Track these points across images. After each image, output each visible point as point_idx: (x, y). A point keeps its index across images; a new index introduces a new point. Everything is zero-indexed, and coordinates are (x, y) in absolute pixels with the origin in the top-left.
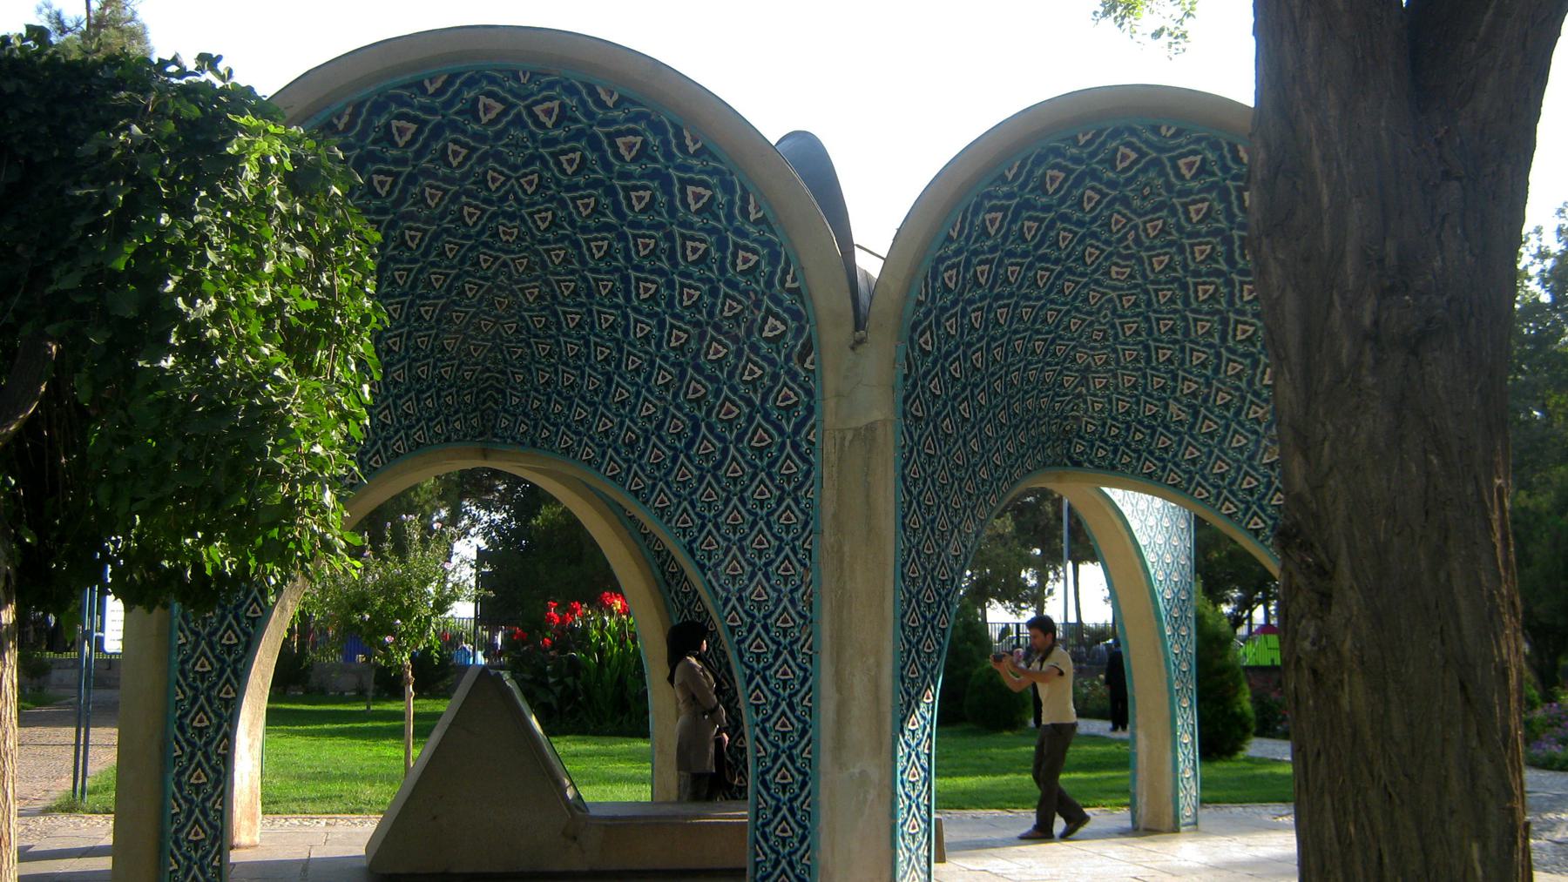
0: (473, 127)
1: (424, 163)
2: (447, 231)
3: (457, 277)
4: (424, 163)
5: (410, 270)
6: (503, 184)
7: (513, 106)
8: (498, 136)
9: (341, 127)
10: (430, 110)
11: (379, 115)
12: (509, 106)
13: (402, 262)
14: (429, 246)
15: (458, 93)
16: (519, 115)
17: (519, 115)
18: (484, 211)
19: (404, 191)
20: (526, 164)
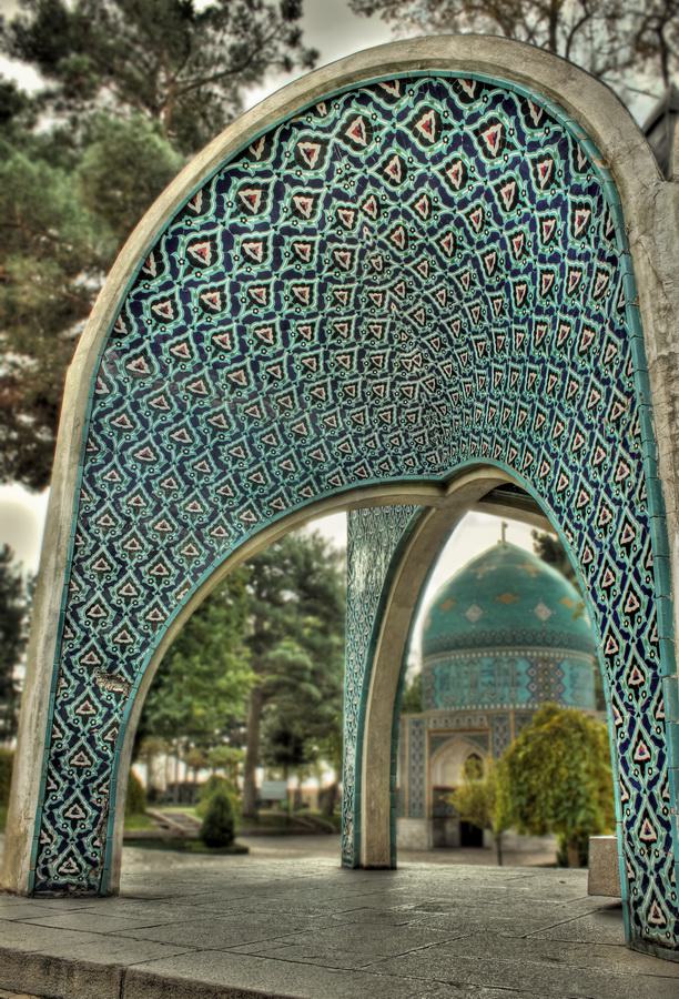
0: (307, 175)
1: (281, 223)
2: (330, 279)
3: (359, 321)
4: (281, 223)
5: (313, 325)
6: (355, 219)
7: (326, 142)
8: (330, 175)
9: (198, 209)
10: (266, 174)
11: (226, 191)
12: (325, 143)
13: (302, 318)
14: (321, 299)
15: (280, 149)
16: (336, 146)
17: (336, 146)
18: (353, 251)
19: (277, 253)
20: (360, 191)
